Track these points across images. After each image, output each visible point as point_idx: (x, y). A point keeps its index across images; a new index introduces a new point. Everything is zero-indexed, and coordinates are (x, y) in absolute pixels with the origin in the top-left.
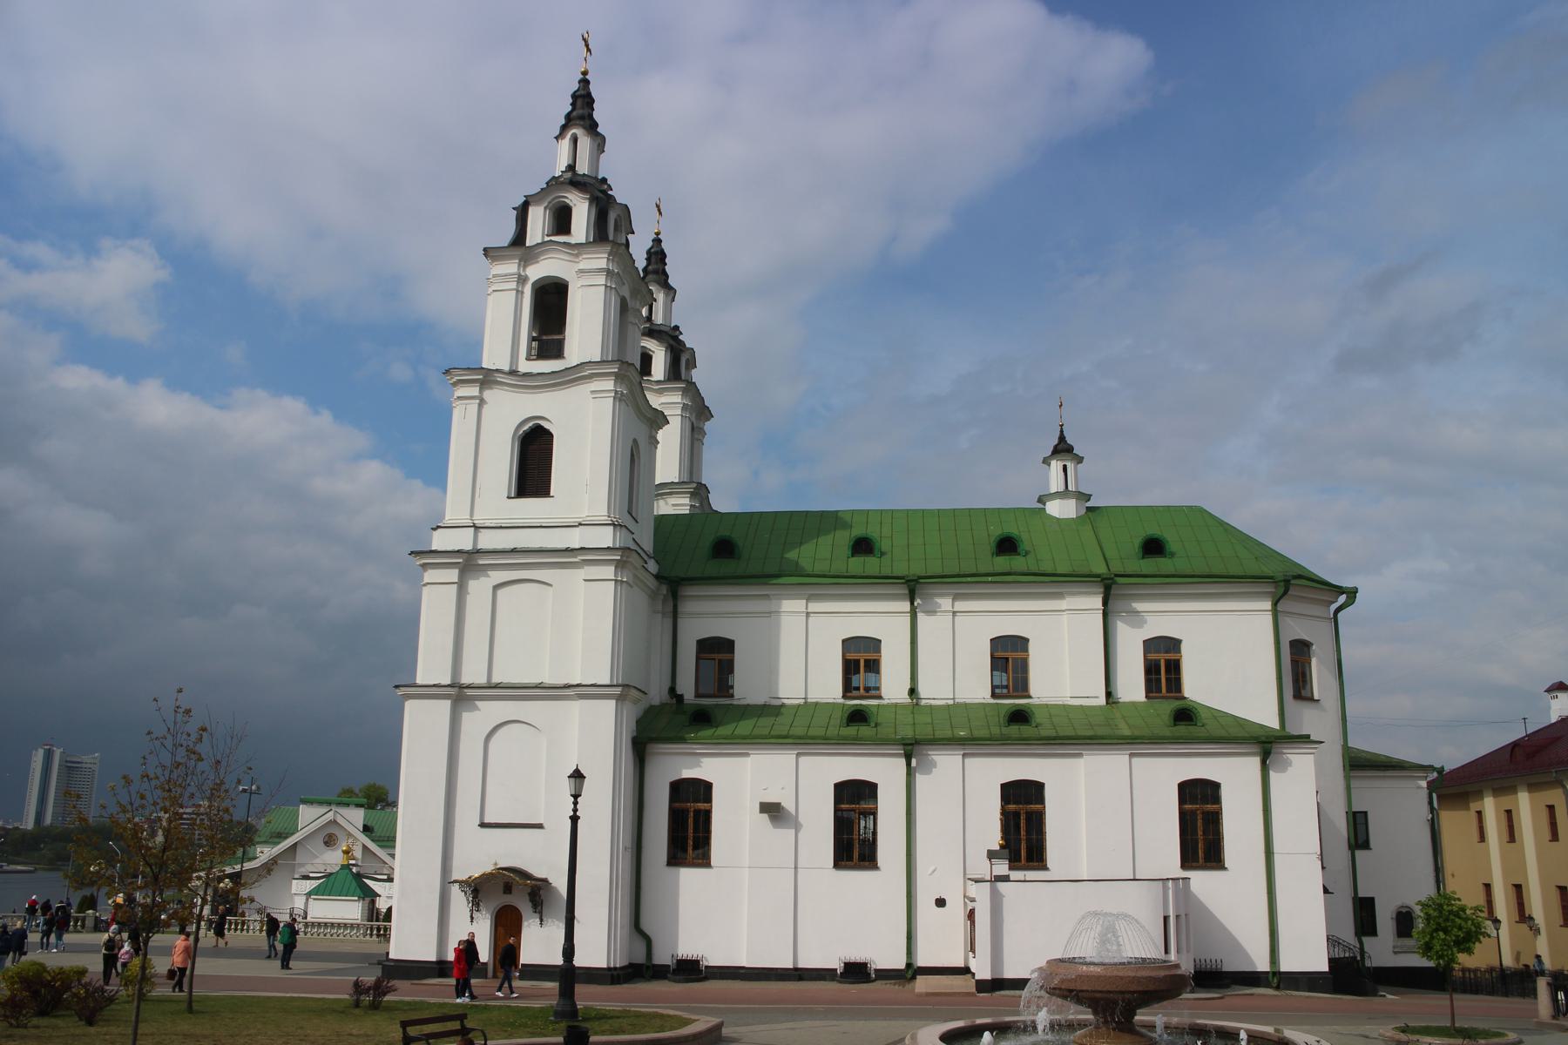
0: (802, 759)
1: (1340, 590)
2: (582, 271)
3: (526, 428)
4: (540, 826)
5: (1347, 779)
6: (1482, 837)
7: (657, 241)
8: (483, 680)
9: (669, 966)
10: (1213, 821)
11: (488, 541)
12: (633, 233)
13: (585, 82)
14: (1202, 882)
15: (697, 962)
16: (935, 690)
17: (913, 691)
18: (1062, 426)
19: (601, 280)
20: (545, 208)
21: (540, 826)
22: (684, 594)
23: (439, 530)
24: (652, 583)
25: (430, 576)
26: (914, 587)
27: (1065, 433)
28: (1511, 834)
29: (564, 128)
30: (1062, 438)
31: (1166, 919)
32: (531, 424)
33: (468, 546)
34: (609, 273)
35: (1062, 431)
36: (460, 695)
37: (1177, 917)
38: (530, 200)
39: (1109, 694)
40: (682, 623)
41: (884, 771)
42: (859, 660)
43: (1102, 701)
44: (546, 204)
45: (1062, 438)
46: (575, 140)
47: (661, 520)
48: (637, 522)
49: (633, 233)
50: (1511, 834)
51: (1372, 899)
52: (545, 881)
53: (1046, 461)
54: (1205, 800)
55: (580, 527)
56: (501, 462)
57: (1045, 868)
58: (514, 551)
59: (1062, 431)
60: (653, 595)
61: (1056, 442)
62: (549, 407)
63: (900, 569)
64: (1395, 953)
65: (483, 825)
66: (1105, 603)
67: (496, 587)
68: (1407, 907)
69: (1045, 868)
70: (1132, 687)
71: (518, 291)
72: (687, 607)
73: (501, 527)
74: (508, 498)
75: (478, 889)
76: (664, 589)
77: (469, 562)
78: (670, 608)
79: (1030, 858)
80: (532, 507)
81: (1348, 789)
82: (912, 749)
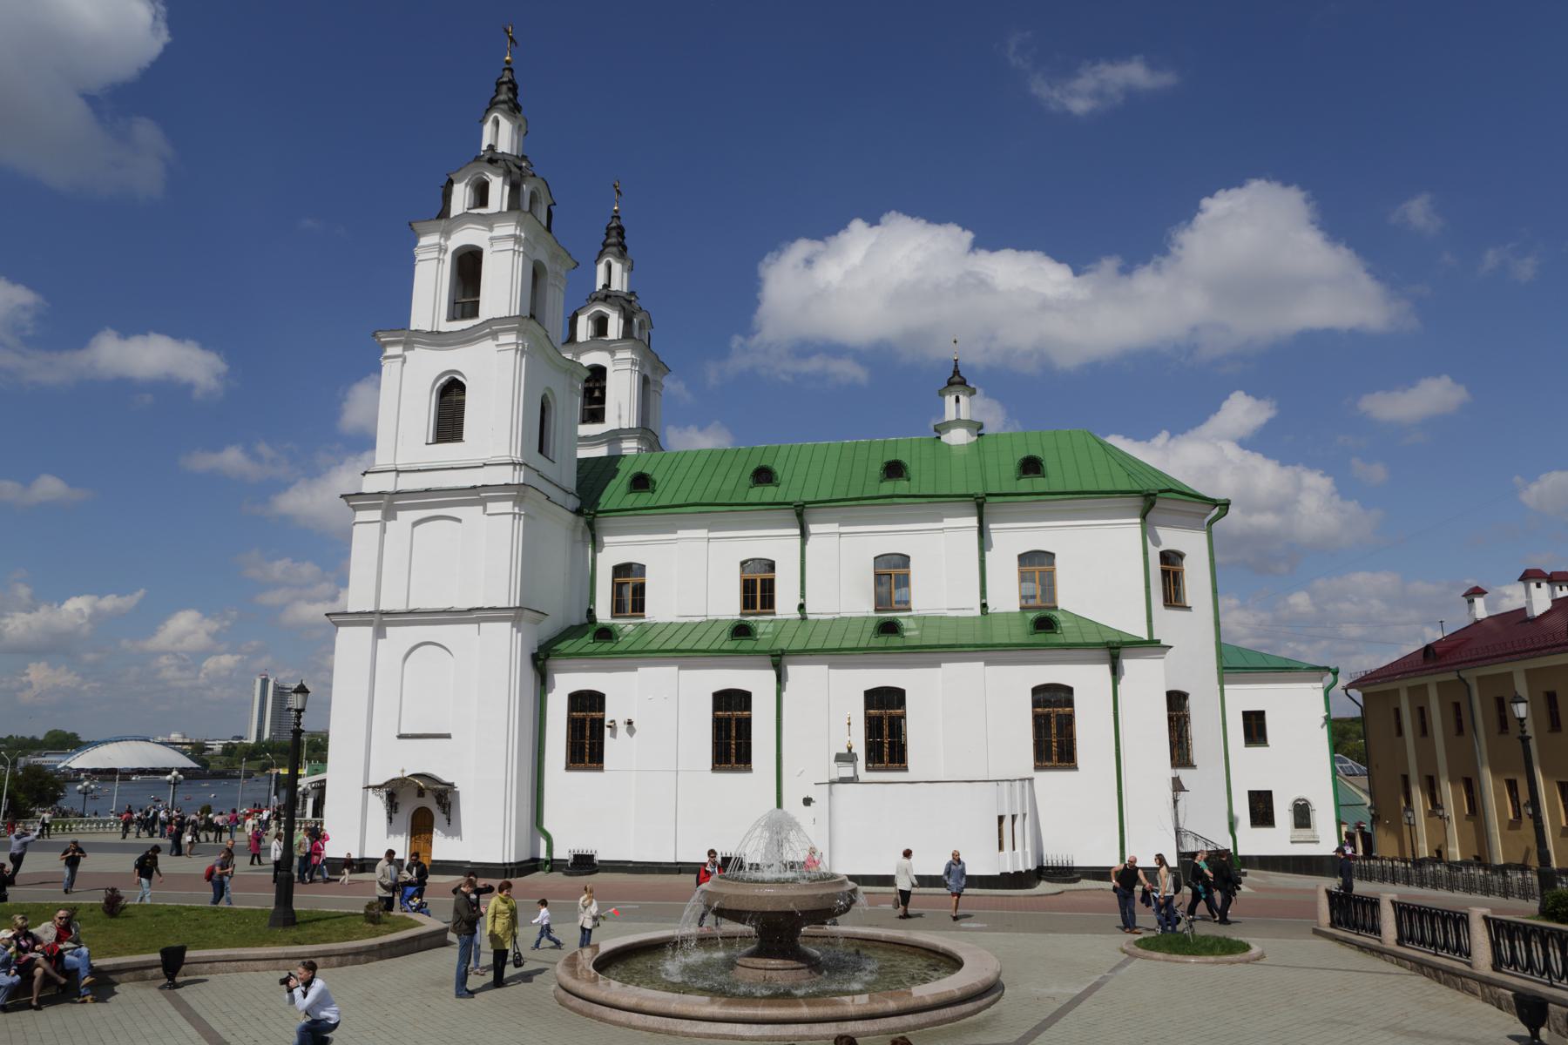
0: (681, 672)
1: (1214, 503)
3: (443, 380)
4: (448, 736)
5: (1222, 682)
6: (1400, 732)
8: (401, 607)
9: (567, 860)
10: (1067, 724)
11: (408, 483)
12: (555, 204)
14: (1051, 782)
15: (592, 857)
19: (510, 245)
20: (466, 185)
21: (448, 736)
23: (367, 475)
25: (361, 516)
26: (801, 515)
28: (1424, 729)
30: (956, 372)
31: (1001, 819)
32: (446, 378)
33: (390, 489)
34: (516, 238)
35: (956, 366)
36: (380, 620)
41: (756, 681)
42: (756, 580)
43: (977, 612)
45: (956, 372)
46: (497, 123)
47: (583, 463)
48: (554, 462)
49: (555, 204)
50: (1424, 729)
51: (1269, 793)
52: (451, 785)
53: (942, 394)
54: (1058, 704)
55: (486, 467)
56: (422, 410)
57: (905, 769)
59: (956, 366)
61: (951, 375)
62: (469, 362)
63: (793, 497)
64: (1292, 842)
65: (401, 737)
66: (981, 521)
67: (416, 524)
68: (1304, 800)
69: (905, 769)
70: (1007, 596)
71: (439, 260)
73: (419, 471)
74: (427, 444)
75: (394, 793)
77: (390, 503)
79: (892, 761)
80: (448, 452)
81: (1222, 690)
82: (778, 661)
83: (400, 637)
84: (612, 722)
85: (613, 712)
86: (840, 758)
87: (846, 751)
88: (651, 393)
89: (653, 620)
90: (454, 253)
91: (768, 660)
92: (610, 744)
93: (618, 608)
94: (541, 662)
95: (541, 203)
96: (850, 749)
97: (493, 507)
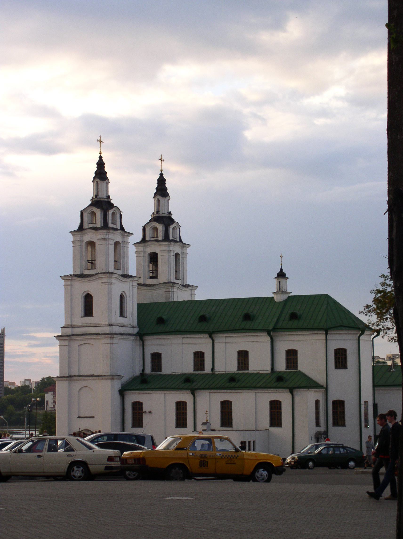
2: (98, 239)
4: (93, 417)
7: (161, 175)
8: (77, 374)
13: (101, 157)
16: (220, 369)
17: (213, 369)
18: (281, 265)
22: (145, 338)
24: (133, 337)
27: (282, 268)
29: (94, 178)
30: (281, 270)
35: (281, 267)
37: (249, 442)
38: (83, 211)
39: (272, 369)
40: (146, 348)
43: (269, 371)
44: (88, 212)
45: (281, 270)
58: (82, 335)
59: (281, 267)
60: (136, 340)
65: (79, 417)
72: (146, 343)
76: (138, 338)
78: (142, 343)
80: (88, 320)
83: (78, 384)
84: (145, 411)
85: (145, 408)
86: (203, 424)
87: (206, 422)
88: (181, 259)
89: (164, 374)
90: (86, 243)
91: (189, 391)
92: (145, 418)
93: (153, 370)
94: (122, 392)
95: (117, 214)
96: (207, 421)
97: (103, 341)
